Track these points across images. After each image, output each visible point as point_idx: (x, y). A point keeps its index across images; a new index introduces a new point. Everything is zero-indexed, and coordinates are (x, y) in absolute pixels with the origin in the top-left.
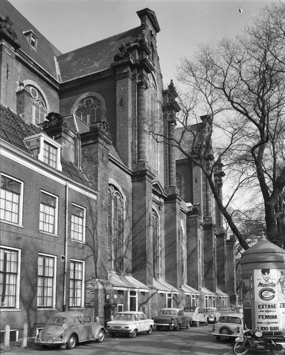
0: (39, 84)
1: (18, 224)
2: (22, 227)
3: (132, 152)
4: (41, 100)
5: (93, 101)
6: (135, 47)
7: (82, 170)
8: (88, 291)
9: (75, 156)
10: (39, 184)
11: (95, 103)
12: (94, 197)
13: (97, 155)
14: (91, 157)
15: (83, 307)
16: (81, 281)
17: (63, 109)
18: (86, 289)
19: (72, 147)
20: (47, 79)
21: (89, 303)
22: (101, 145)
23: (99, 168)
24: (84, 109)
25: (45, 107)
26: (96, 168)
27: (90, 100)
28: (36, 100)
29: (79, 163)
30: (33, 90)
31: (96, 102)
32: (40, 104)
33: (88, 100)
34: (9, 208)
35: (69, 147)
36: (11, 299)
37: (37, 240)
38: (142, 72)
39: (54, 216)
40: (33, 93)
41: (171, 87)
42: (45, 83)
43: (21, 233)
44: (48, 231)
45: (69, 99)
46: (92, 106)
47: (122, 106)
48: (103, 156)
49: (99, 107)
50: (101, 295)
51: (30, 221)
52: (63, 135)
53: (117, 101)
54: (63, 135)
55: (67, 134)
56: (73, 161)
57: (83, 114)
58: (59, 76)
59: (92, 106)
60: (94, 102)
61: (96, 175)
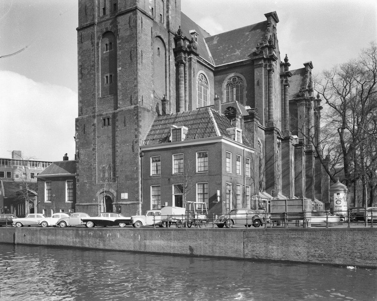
0: (204, 71)
2: (232, 173)
3: (265, 115)
5: (237, 79)
17: (217, 83)
19: (240, 124)
20: (209, 66)
24: (232, 84)
27: (235, 78)
30: (202, 76)
38: (271, 63)
41: (286, 60)
42: (207, 69)
45: (222, 76)
46: (237, 83)
47: (259, 85)
49: (242, 83)
53: (255, 82)
54: (236, 118)
55: (237, 117)
58: (211, 57)
59: (237, 83)
60: (238, 80)
61: (253, 139)
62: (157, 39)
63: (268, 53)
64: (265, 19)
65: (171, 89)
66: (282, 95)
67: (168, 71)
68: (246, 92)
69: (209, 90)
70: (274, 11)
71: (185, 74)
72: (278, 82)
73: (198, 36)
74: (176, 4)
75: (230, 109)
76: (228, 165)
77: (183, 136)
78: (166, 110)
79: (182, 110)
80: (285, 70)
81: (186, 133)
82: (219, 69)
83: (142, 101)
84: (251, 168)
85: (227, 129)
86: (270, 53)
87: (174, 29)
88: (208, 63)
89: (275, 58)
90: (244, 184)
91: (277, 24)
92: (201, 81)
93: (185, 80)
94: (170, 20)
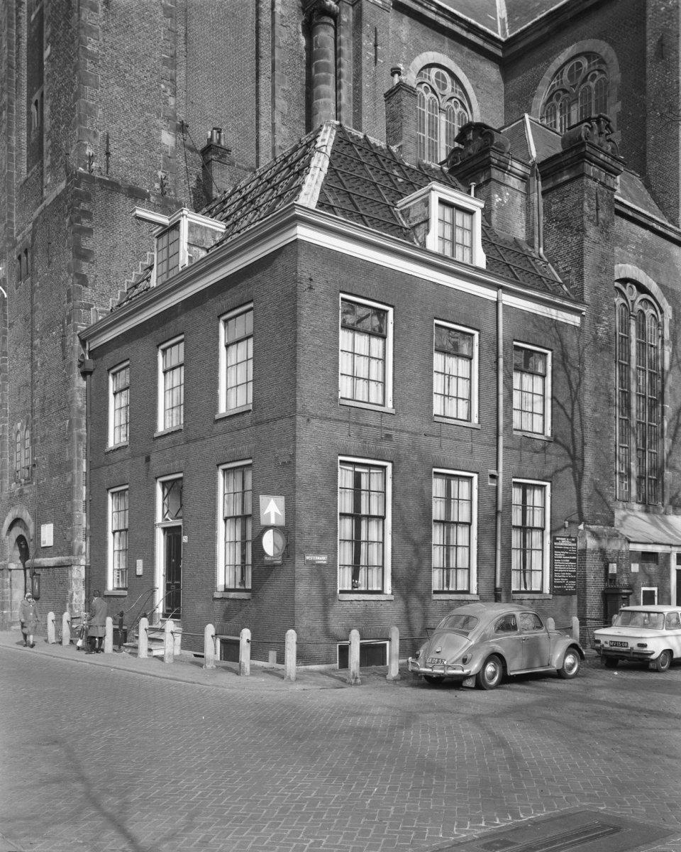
0: (451, 57)
1: (383, 405)
4: (458, 97)
5: (585, 64)
7: (545, 254)
8: (558, 555)
9: (528, 222)
10: (430, 307)
11: (592, 68)
13: (582, 209)
14: (567, 219)
15: (548, 592)
16: (542, 529)
17: (513, 104)
18: (553, 549)
19: (519, 200)
20: (471, 37)
21: (564, 584)
22: (590, 181)
23: (586, 244)
24: (565, 91)
25: (468, 110)
26: (581, 243)
27: (579, 65)
28: (447, 97)
29: (537, 239)
30: (437, 75)
31: (594, 64)
32: (456, 107)
33: (573, 66)
34: (362, 372)
35: (511, 202)
36: (374, 575)
37: (428, 438)
39: (470, 379)
40: (438, 83)
42: (466, 49)
43: (392, 425)
44: (455, 416)
45: (529, 74)
46: (585, 80)
47: (663, 58)
48: (597, 210)
49: (603, 76)
50: (593, 565)
51: (410, 395)
52: (496, 174)
53: (648, 49)
54: (496, 174)
55: (503, 168)
56: (521, 234)
57: (561, 105)
59: (585, 80)
60: (589, 67)
61: (579, 263)
65: (278, 120)
67: (265, 51)
71: (338, 54)
75: (470, 136)
82: (520, 46)
84: (553, 398)
90: (497, 469)
92: (434, 92)
93: (338, 76)
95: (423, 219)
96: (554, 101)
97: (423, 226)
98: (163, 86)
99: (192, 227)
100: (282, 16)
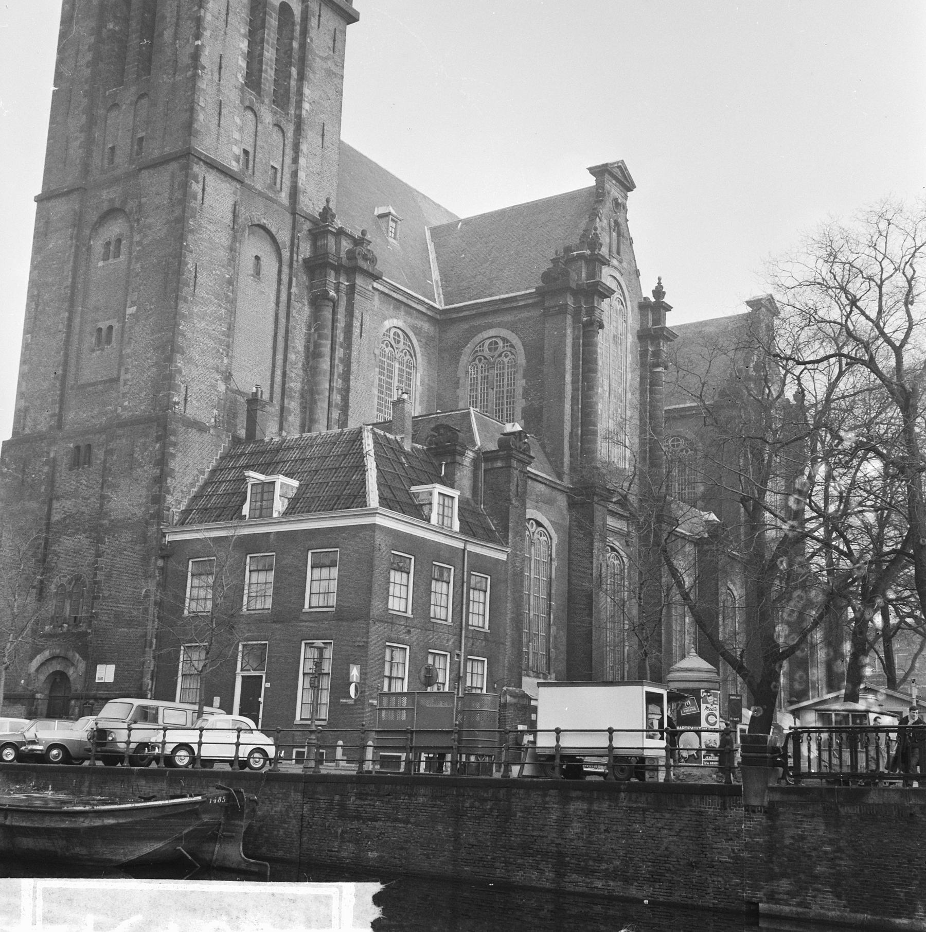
1: (406, 612)
5: (501, 344)
6: (581, 257)
12: (503, 557)
24: (485, 358)
27: (496, 343)
28: (400, 350)
30: (395, 334)
38: (593, 302)
41: (659, 292)
46: (500, 356)
49: (513, 356)
57: (482, 367)
59: (500, 356)
60: (504, 347)
62: (253, 233)
63: (584, 275)
64: (591, 181)
66: (643, 392)
68: (524, 381)
69: (419, 375)
70: (620, 159)
72: (629, 356)
73: (399, 222)
74: (323, 140)
76: (394, 590)
77: (279, 505)
78: (258, 428)
79: (321, 429)
80: (655, 322)
81: (291, 494)
83: (183, 402)
85: (414, 489)
86: (592, 274)
87: (312, 204)
88: (416, 298)
89: (604, 288)
91: (629, 194)
92: (392, 346)
94: (300, 184)
95: (428, 502)
96: (477, 361)
97: (428, 506)
98: (221, 350)
99: (282, 485)
100: (296, 294)
